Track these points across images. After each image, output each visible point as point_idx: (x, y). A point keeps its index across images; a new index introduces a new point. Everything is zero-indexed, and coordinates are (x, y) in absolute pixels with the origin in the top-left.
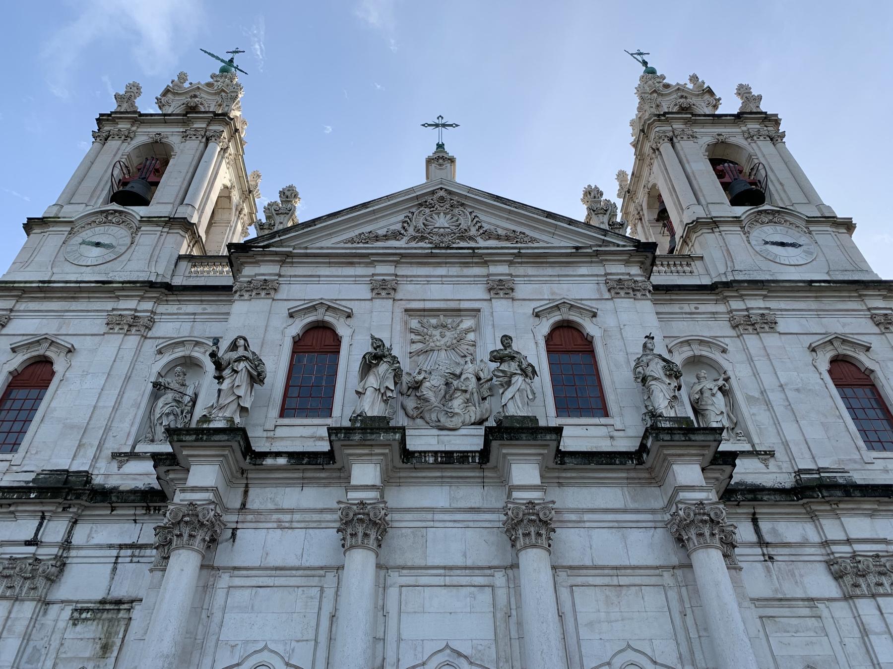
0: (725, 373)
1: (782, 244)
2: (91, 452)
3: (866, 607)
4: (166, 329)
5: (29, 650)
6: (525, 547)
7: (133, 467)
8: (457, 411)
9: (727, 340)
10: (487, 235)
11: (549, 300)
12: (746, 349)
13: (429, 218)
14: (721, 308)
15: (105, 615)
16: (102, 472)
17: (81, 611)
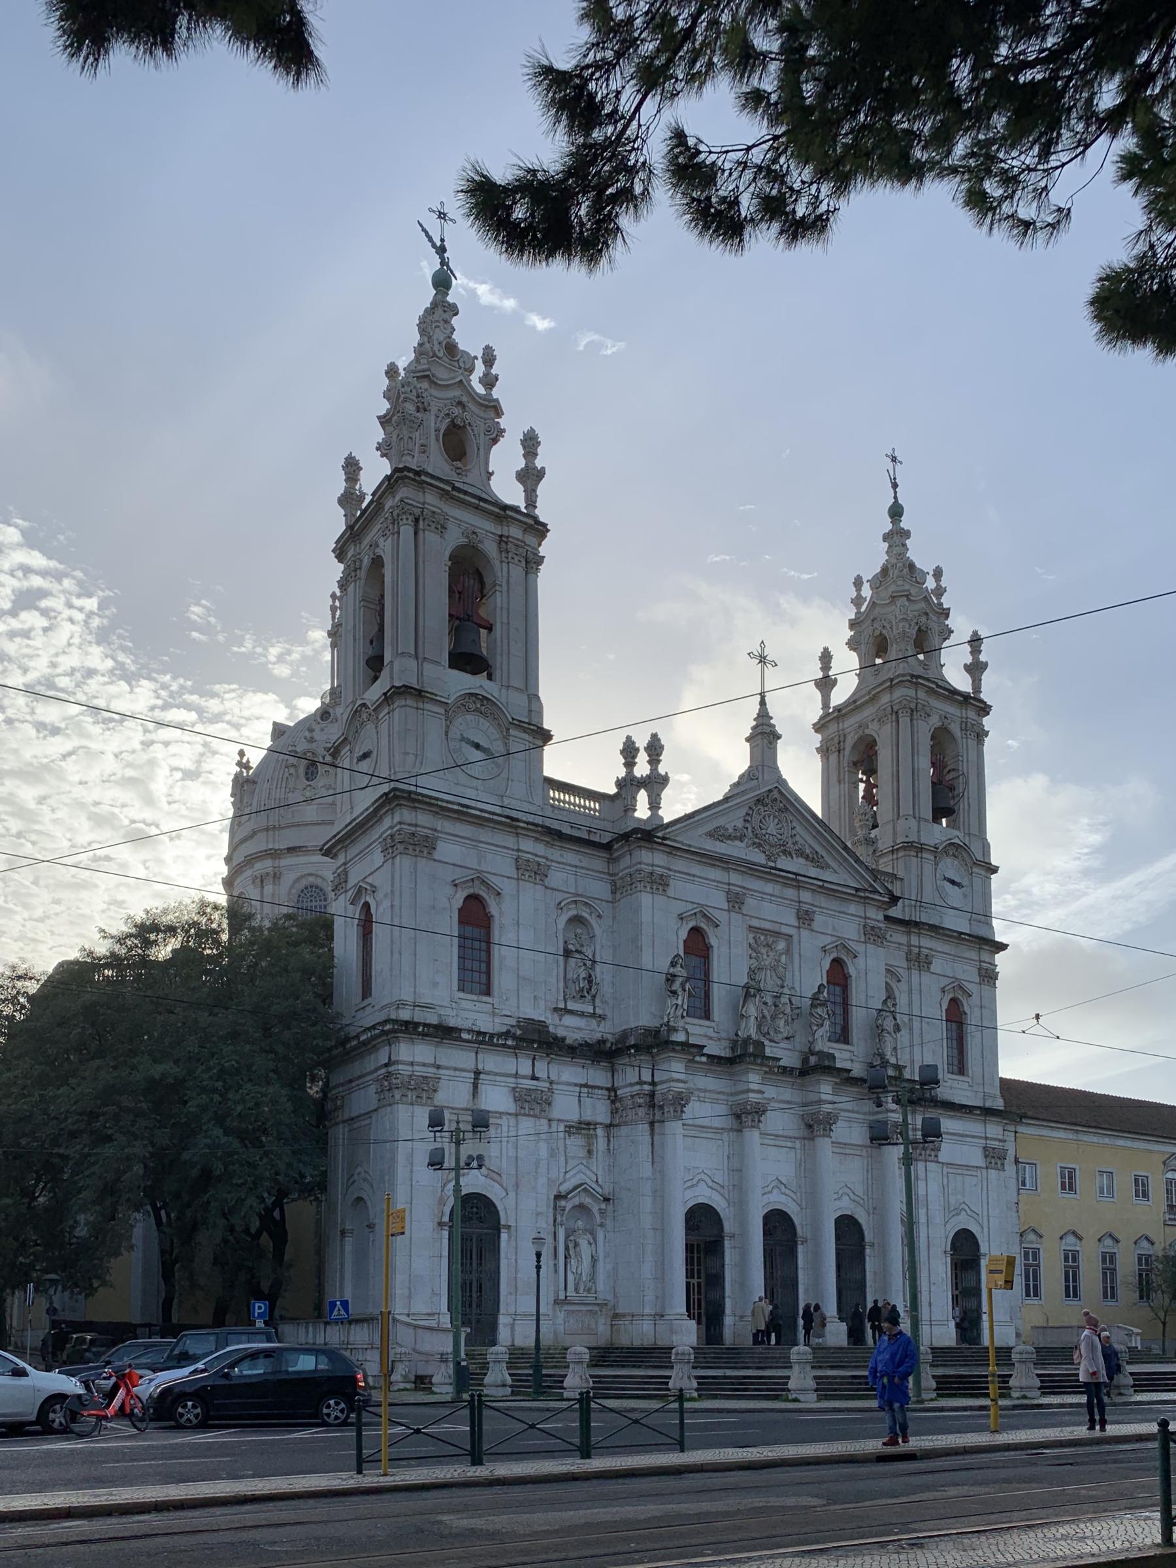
0: (895, 998)
2: (542, 1004)
4: (557, 878)
7: (569, 1020)
8: (782, 1030)
9: (901, 971)
10: (801, 853)
11: (832, 935)
12: (910, 982)
14: (903, 939)
15: (583, 1131)
17: (570, 1127)
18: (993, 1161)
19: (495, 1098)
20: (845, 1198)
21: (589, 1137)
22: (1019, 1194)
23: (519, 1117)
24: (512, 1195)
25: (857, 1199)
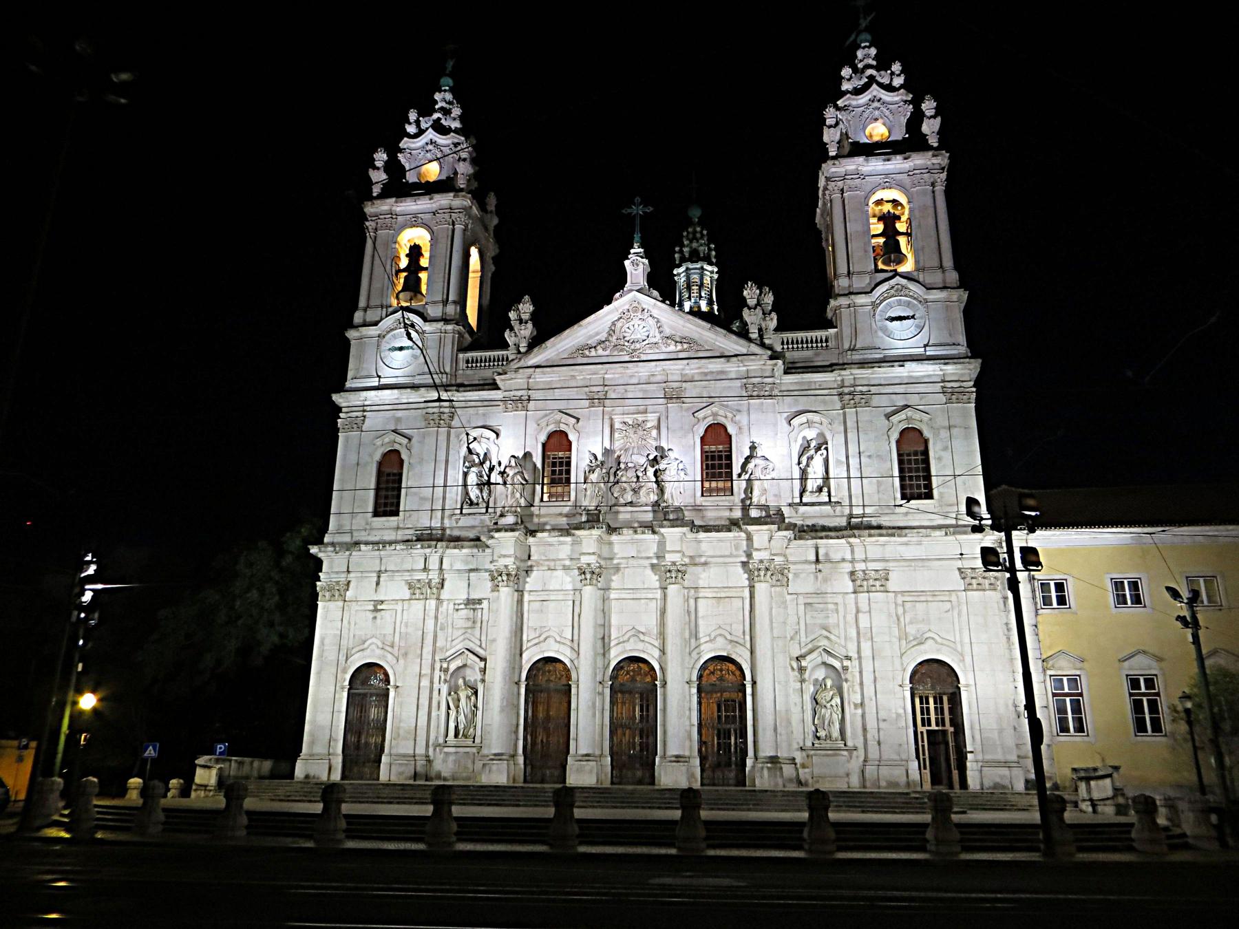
1: (900, 318)
3: (863, 597)
5: (439, 624)
6: (670, 584)
13: (627, 330)
16: (448, 526)
17: (459, 604)
18: (974, 581)
19: (395, 589)
20: (719, 639)
21: (474, 610)
22: (1037, 614)
23: (412, 601)
24: (401, 661)
25: (735, 639)
